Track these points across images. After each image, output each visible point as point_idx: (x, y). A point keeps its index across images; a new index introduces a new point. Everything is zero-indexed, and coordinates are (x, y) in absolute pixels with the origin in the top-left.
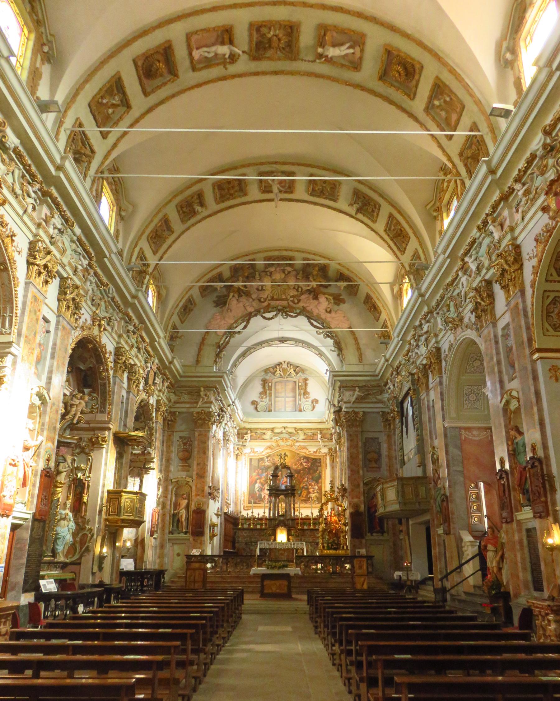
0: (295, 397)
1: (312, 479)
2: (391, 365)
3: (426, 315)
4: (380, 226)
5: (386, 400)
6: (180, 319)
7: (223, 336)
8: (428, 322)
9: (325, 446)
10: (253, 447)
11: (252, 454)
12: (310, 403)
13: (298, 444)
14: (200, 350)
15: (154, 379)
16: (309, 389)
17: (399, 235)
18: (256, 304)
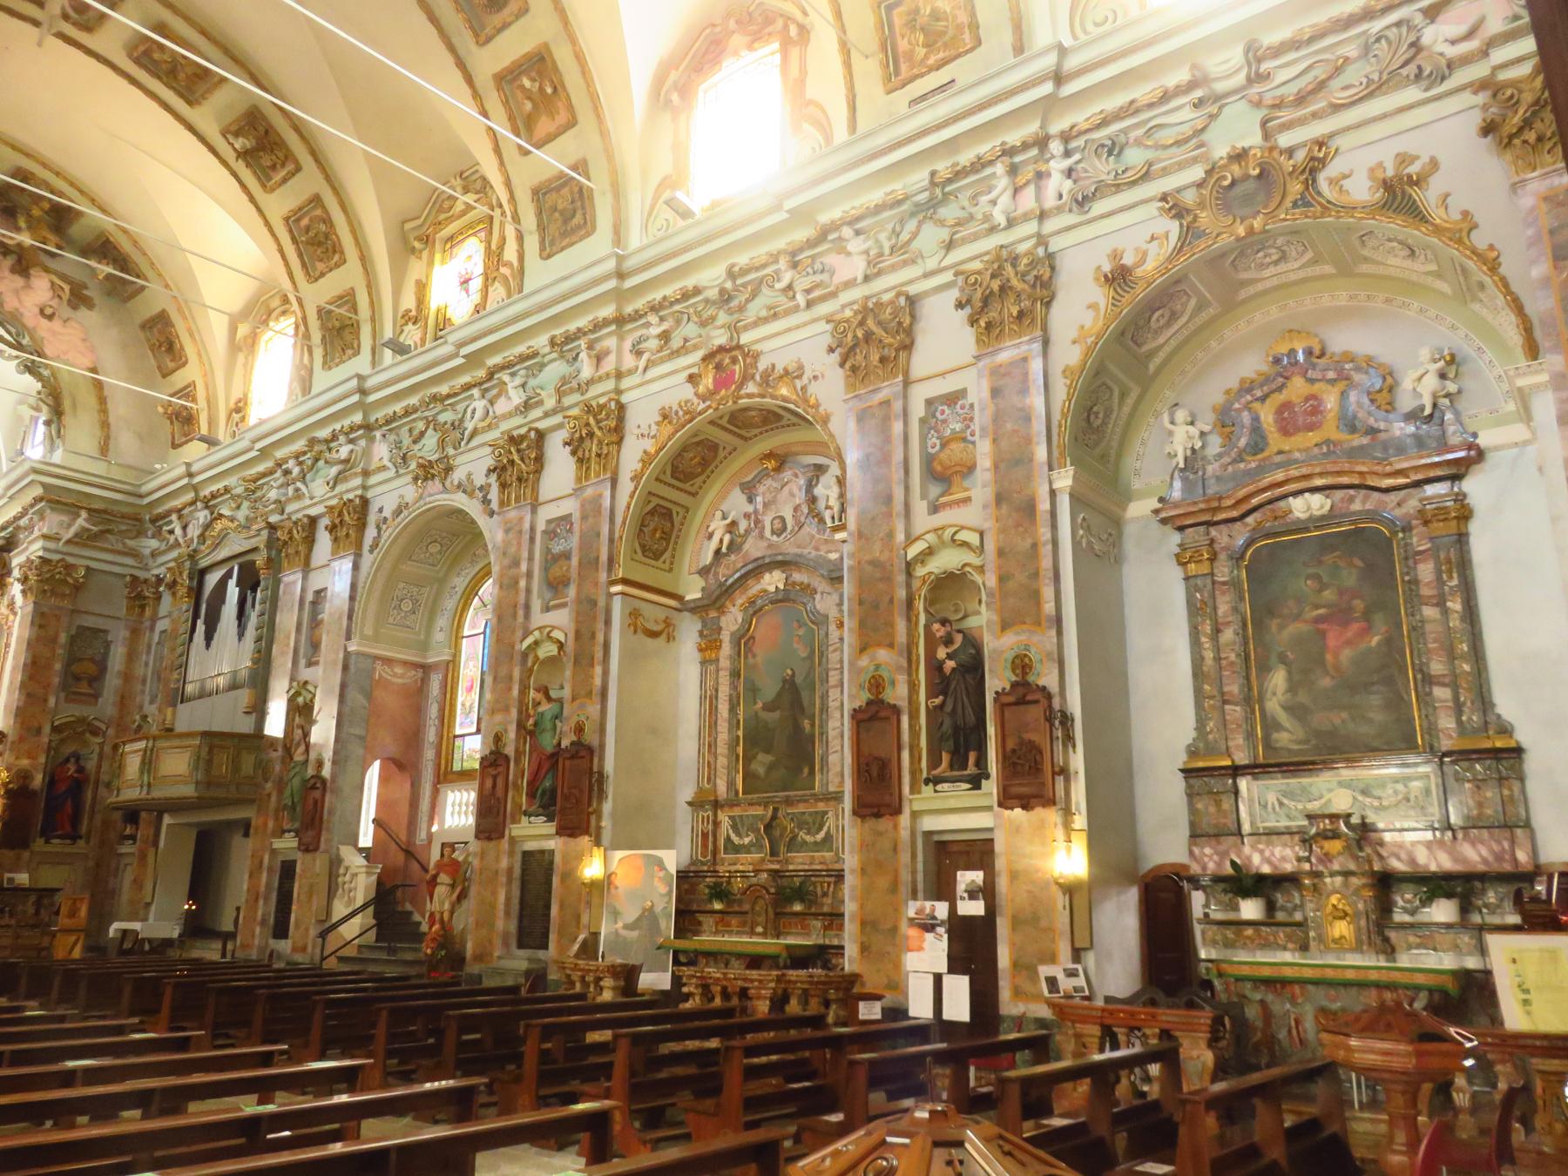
2: (195, 488)
3: (352, 429)
4: (280, 203)
5: (147, 552)
8: (351, 441)
17: (320, 244)
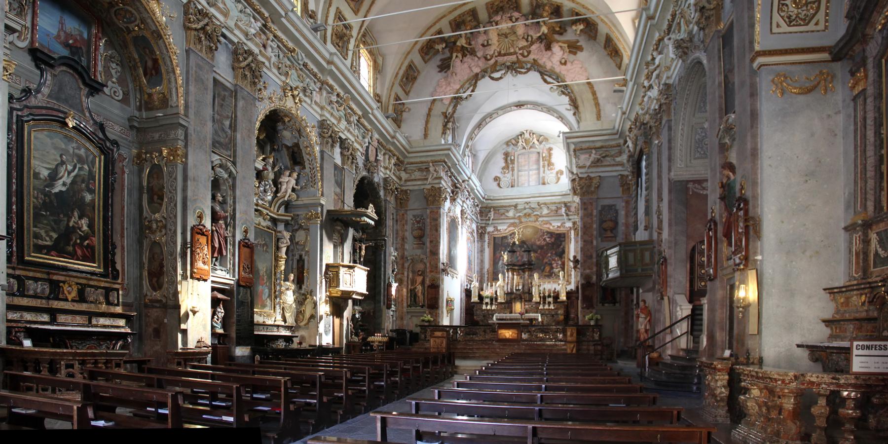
0: (538, 169)
6: (404, 90)
7: (450, 104)
12: (554, 175)
13: (541, 219)
14: (427, 122)
15: (377, 155)
16: (553, 160)
18: (482, 64)
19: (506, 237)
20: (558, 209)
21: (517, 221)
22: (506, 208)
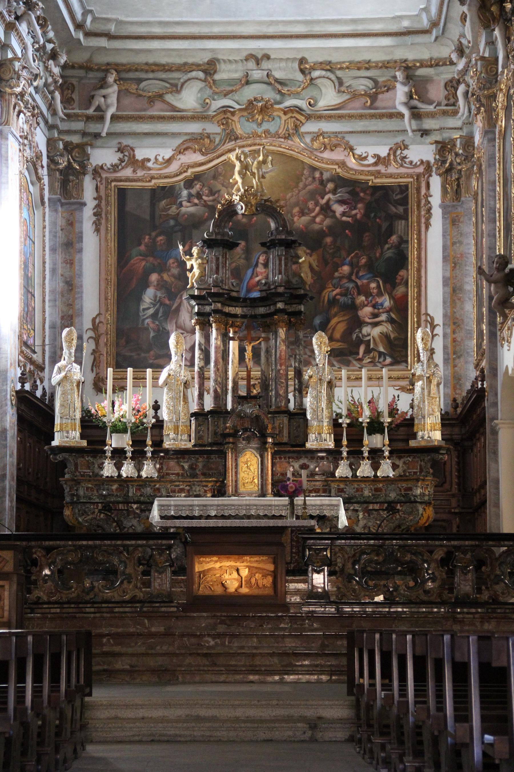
1: (370, 267)
9: (425, 133)
10: (126, 141)
11: (128, 172)
19: (168, 192)
20: (380, 89)
21: (213, 128)
22: (174, 74)
